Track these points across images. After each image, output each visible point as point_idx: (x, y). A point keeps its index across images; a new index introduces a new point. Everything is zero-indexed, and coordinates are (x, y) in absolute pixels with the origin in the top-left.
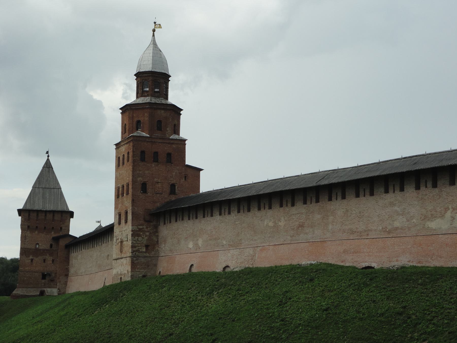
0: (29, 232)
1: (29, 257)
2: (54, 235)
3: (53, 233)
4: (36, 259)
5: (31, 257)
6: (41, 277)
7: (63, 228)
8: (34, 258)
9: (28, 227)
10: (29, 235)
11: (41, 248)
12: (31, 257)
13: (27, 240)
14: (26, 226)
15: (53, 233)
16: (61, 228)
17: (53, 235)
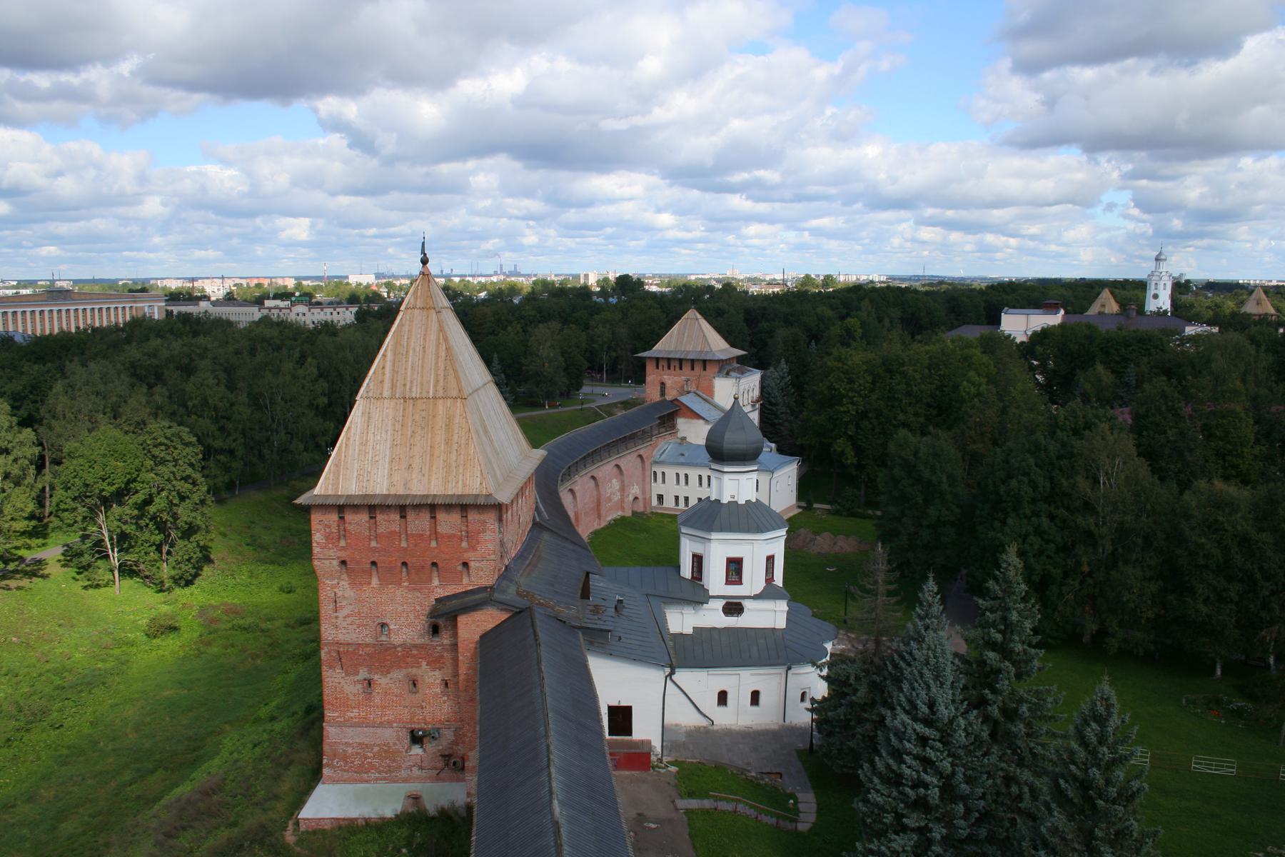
0: (345, 584)
1: (357, 673)
2: (441, 593)
3: (436, 582)
4: (382, 681)
5: (363, 674)
6: (407, 740)
7: (472, 564)
8: (376, 677)
9: (344, 563)
10: (350, 593)
11: (397, 639)
12: (363, 674)
13: (341, 614)
14: (335, 563)
15: (436, 582)
16: (465, 564)
17: (439, 589)
